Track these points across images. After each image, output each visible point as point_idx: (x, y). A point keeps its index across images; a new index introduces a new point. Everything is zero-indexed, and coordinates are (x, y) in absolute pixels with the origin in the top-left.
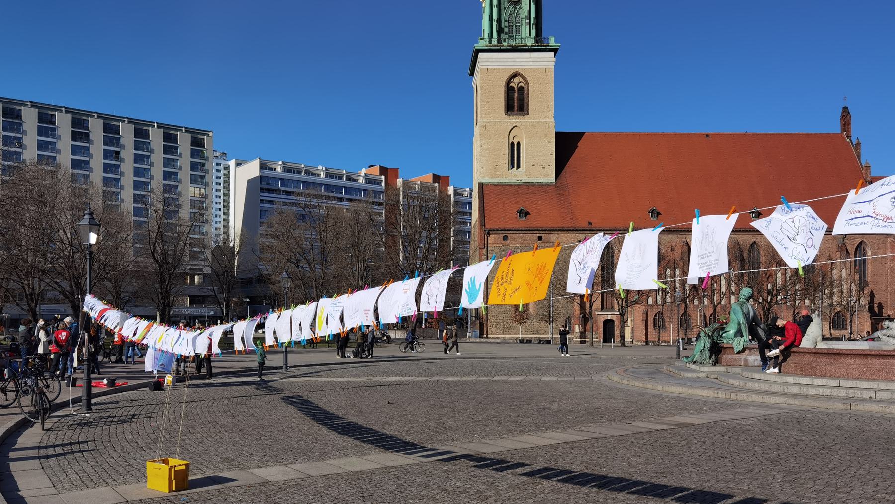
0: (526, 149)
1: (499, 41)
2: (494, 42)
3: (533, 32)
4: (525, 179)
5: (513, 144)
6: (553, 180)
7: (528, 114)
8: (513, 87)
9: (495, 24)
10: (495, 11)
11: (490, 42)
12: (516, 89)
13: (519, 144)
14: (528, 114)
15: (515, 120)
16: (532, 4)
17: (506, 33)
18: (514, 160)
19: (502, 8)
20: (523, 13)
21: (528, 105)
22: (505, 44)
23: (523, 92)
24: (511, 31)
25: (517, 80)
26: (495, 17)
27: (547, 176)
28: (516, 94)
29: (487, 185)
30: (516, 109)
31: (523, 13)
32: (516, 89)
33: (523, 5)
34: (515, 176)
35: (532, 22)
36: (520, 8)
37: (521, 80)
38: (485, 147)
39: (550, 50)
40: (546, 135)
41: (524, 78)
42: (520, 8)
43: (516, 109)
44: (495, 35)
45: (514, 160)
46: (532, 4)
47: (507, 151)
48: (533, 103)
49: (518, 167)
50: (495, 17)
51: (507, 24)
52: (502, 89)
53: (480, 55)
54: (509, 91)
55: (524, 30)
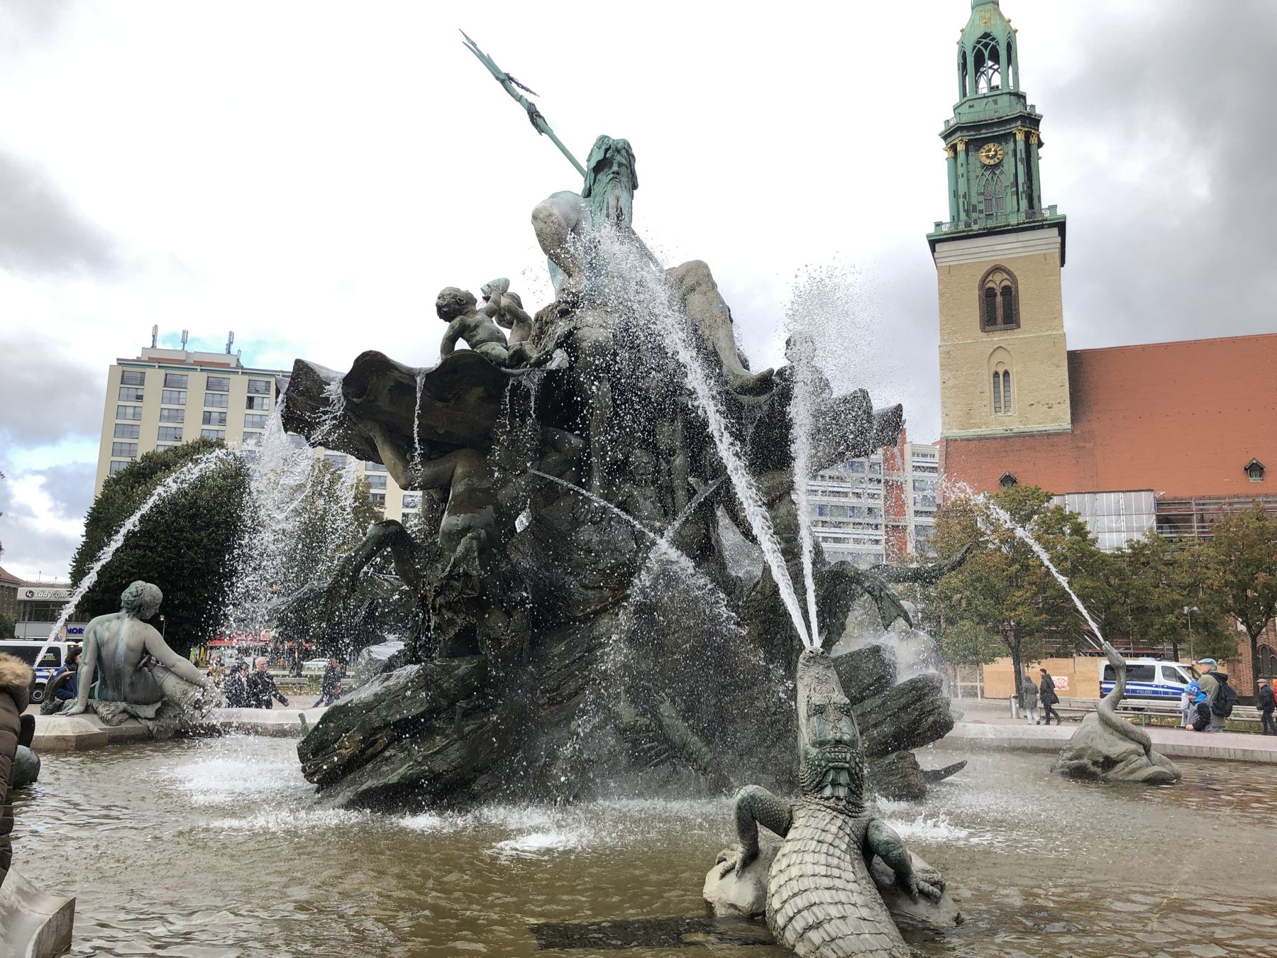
1: (968, 225)
2: (962, 227)
3: (1024, 204)
4: (1018, 427)
6: (1066, 424)
9: (961, 200)
10: (962, 182)
12: (998, 291)
13: (1006, 373)
15: (998, 338)
17: (981, 212)
19: (972, 175)
24: (989, 207)
25: (998, 277)
26: (961, 193)
27: (1055, 420)
28: (999, 299)
32: (998, 291)
33: (1006, 167)
35: (1020, 189)
36: (1002, 173)
37: (1006, 276)
38: (951, 383)
39: (1051, 226)
41: (1009, 273)
42: (1002, 173)
44: (963, 216)
46: (1019, 164)
50: (961, 193)
51: (981, 198)
52: (976, 292)
54: (988, 295)
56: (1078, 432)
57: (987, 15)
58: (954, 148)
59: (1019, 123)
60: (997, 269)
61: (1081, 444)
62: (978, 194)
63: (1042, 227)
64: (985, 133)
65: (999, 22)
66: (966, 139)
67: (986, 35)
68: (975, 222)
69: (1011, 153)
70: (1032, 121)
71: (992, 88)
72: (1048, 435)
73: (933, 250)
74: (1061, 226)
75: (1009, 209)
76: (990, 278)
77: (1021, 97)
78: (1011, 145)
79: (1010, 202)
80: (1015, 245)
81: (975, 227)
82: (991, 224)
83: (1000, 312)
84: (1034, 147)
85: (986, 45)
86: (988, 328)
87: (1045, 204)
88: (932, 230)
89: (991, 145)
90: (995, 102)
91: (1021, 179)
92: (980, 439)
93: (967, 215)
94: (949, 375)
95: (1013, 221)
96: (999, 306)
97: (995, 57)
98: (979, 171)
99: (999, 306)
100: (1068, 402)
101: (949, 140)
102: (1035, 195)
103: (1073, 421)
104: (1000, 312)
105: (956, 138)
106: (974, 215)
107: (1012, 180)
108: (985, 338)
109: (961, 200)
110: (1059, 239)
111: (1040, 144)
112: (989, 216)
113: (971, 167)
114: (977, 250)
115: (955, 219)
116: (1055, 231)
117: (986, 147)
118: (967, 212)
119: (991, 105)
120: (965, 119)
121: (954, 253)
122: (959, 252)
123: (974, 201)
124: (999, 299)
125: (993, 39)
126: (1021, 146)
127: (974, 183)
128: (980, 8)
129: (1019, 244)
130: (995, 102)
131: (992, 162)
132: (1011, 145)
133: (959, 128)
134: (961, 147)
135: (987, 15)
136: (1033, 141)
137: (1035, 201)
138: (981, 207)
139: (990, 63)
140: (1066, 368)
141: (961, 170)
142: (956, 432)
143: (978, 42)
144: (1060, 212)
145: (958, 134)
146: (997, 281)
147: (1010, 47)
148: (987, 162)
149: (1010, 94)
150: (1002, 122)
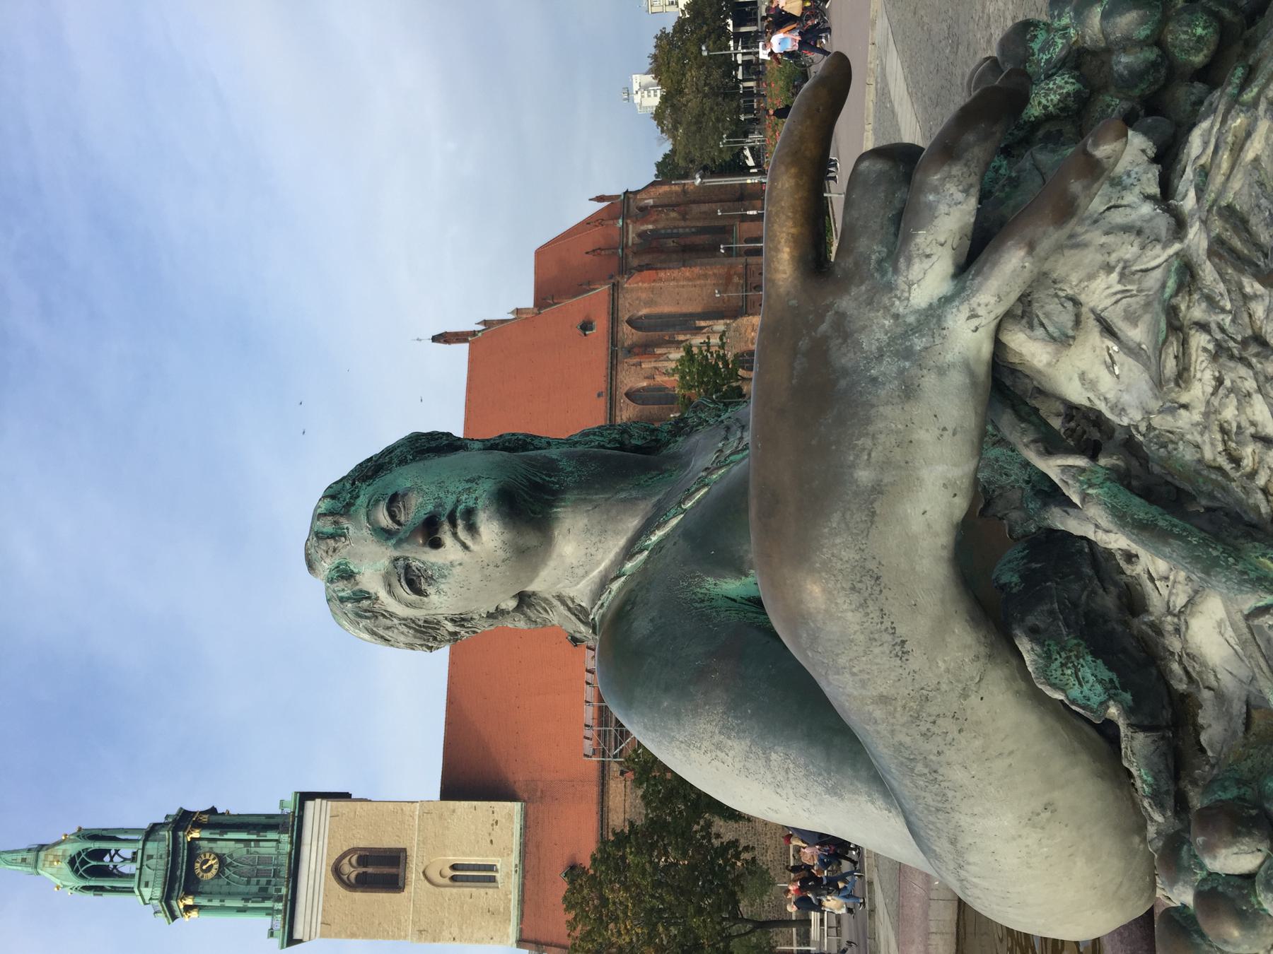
0: (464, 854)
1: (279, 899)
2: (280, 906)
3: (272, 835)
4: (514, 858)
5: (453, 878)
6: (516, 806)
7: (405, 850)
8: (358, 876)
9: (250, 905)
10: (228, 903)
11: (278, 911)
12: (361, 870)
13: (454, 867)
14: (405, 850)
16: (226, 837)
17: (269, 882)
18: (482, 875)
19: (225, 889)
20: (240, 850)
21: (390, 850)
22: (284, 891)
23: (367, 857)
24: (265, 874)
26: (240, 904)
27: (510, 817)
28: (370, 870)
29: (521, 931)
30: (393, 870)
31: (240, 850)
32: (361, 870)
33: (226, 851)
34: (508, 875)
35: (254, 837)
36: (231, 856)
37: (346, 861)
38: (455, 931)
39: (302, 807)
40: (441, 816)
42: (231, 856)
43: (393, 870)
44: (268, 904)
45: (482, 875)
46: (226, 837)
47: (465, 891)
48: (388, 841)
49: (491, 868)
50: (240, 904)
51: (254, 880)
52: (360, 896)
53: (297, 936)
54: (364, 883)
55: (267, 849)
56: (525, 796)
57: (51, 858)
58: (188, 909)
59: (181, 834)
60: (337, 871)
61: (539, 794)
62: (248, 883)
63: (301, 819)
64: (182, 873)
65: (62, 847)
66: (182, 894)
67: (72, 862)
68: (280, 890)
69: (212, 845)
70: (184, 820)
71: (133, 859)
72: (525, 829)
73: (300, 941)
74: (305, 797)
75: (273, 851)
76: (345, 877)
77: (154, 828)
78: (204, 844)
79: (267, 849)
80: (314, 848)
81: (284, 891)
82: (284, 873)
83: (386, 870)
84: (214, 818)
85: (83, 863)
86: (401, 884)
87: (276, 810)
88: (276, 942)
89: (197, 865)
90: (150, 857)
91: (244, 836)
92: (522, 901)
93: (268, 898)
94: (446, 934)
95: (286, 848)
96: (378, 870)
97: (99, 854)
98: (223, 881)
99: (378, 870)
100: (493, 803)
101: (178, 913)
102: (264, 820)
103: (511, 797)
104: (386, 870)
105: (179, 905)
106: (272, 890)
107: (241, 845)
108: (410, 889)
109: (250, 905)
110: (318, 801)
111: (213, 811)
112: (276, 874)
113: (216, 889)
114: (310, 891)
115: (270, 912)
116: (309, 805)
117: (198, 871)
118: (264, 899)
119: (152, 862)
120: (158, 893)
121: (308, 918)
122: (309, 912)
123: (255, 889)
124: (370, 870)
125: (79, 854)
126: (206, 834)
127: (233, 890)
128: (40, 864)
129: (314, 843)
130: (150, 857)
131: (216, 866)
132: (204, 844)
133: (167, 898)
134: (189, 901)
135: (51, 858)
136: (205, 818)
137: (272, 821)
138: (263, 881)
139: (107, 858)
140: (457, 803)
141: (216, 903)
142: (512, 931)
143: (76, 871)
144: (290, 799)
145: (174, 903)
146: (350, 871)
147: (94, 836)
148: (214, 871)
149: (145, 841)
150: (174, 852)
